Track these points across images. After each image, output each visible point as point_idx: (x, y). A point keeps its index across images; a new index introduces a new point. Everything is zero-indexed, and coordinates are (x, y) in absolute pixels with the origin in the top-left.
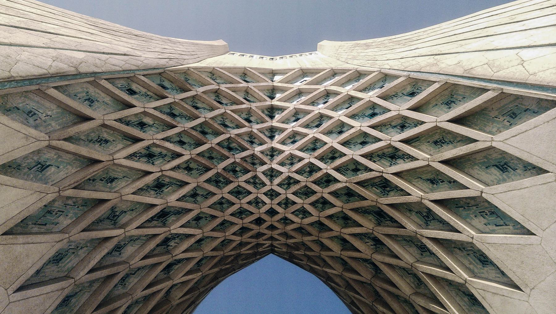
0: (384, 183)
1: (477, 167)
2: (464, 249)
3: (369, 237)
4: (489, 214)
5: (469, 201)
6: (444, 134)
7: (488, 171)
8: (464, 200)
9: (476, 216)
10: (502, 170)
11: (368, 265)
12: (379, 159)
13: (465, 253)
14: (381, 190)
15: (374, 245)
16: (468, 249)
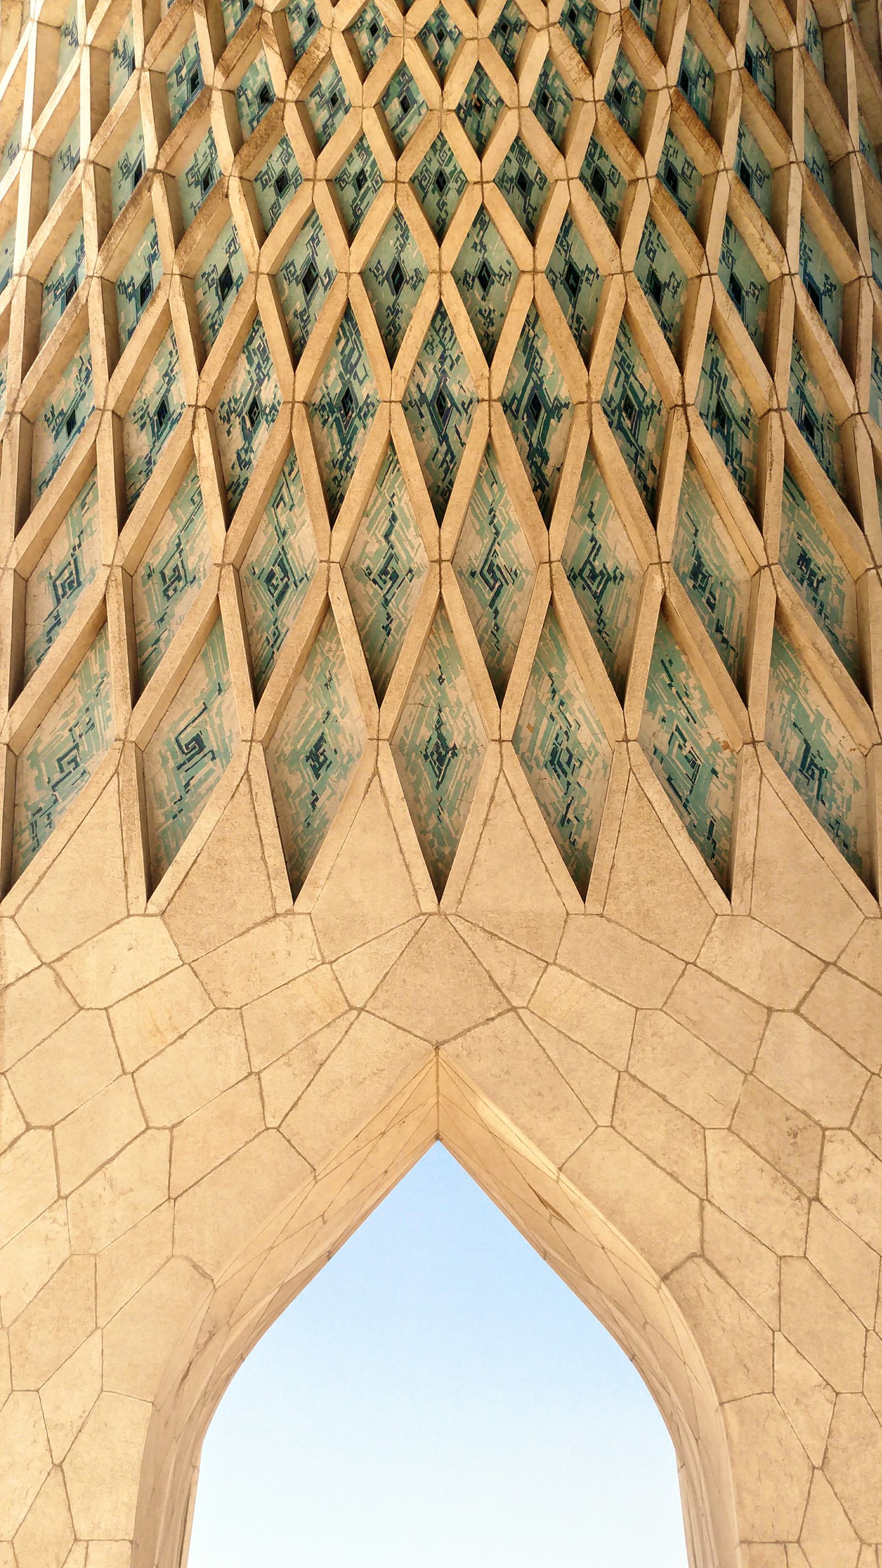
0: (640, 404)
1: (787, 698)
2: (562, 703)
3: (444, 372)
4: (685, 752)
5: (696, 694)
6: (834, 581)
7: (789, 730)
8: (692, 682)
9: (663, 720)
10: (803, 765)
11: (334, 374)
12: (708, 369)
13: (552, 708)
14: (617, 399)
15: (423, 396)
16: (568, 715)
